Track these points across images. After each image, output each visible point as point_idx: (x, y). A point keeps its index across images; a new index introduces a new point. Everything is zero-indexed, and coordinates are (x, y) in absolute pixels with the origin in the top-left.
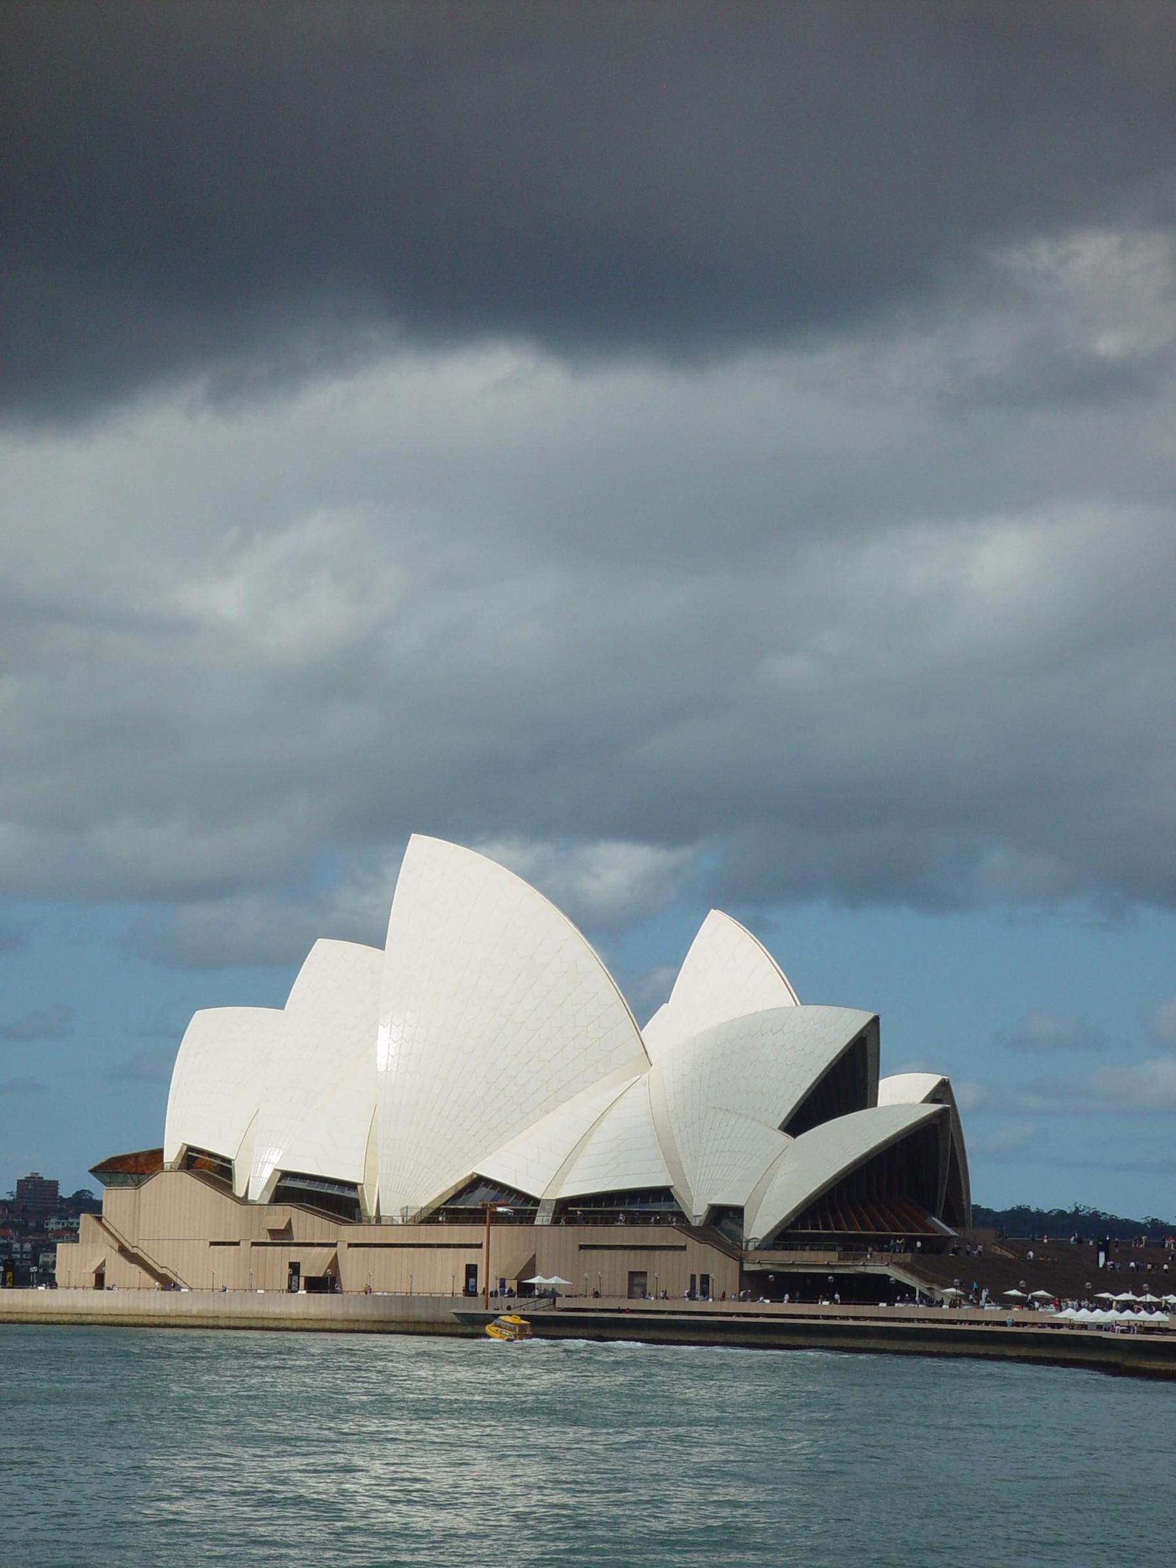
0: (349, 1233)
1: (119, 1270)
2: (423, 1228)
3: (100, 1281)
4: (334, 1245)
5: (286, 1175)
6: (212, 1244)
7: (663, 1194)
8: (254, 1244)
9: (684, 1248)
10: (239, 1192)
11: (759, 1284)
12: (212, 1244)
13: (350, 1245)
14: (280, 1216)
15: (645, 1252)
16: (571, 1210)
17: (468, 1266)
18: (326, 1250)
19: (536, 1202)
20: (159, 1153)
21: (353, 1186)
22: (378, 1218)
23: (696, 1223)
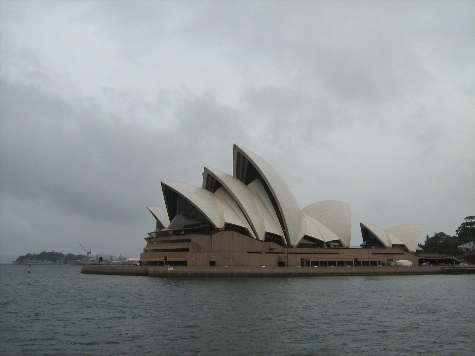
2: (297, 249)
3: (213, 264)
4: (284, 253)
5: (267, 234)
6: (248, 252)
7: (338, 241)
8: (267, 253)
9: (403, 254)
10: (255, 238)
12: (248, 252)
13: (288, 253)
14: (273, 245)
15: (384, 255)
17: (301, 258)
18: (282, 255)
22: (289, 246)
23: (389, 248)
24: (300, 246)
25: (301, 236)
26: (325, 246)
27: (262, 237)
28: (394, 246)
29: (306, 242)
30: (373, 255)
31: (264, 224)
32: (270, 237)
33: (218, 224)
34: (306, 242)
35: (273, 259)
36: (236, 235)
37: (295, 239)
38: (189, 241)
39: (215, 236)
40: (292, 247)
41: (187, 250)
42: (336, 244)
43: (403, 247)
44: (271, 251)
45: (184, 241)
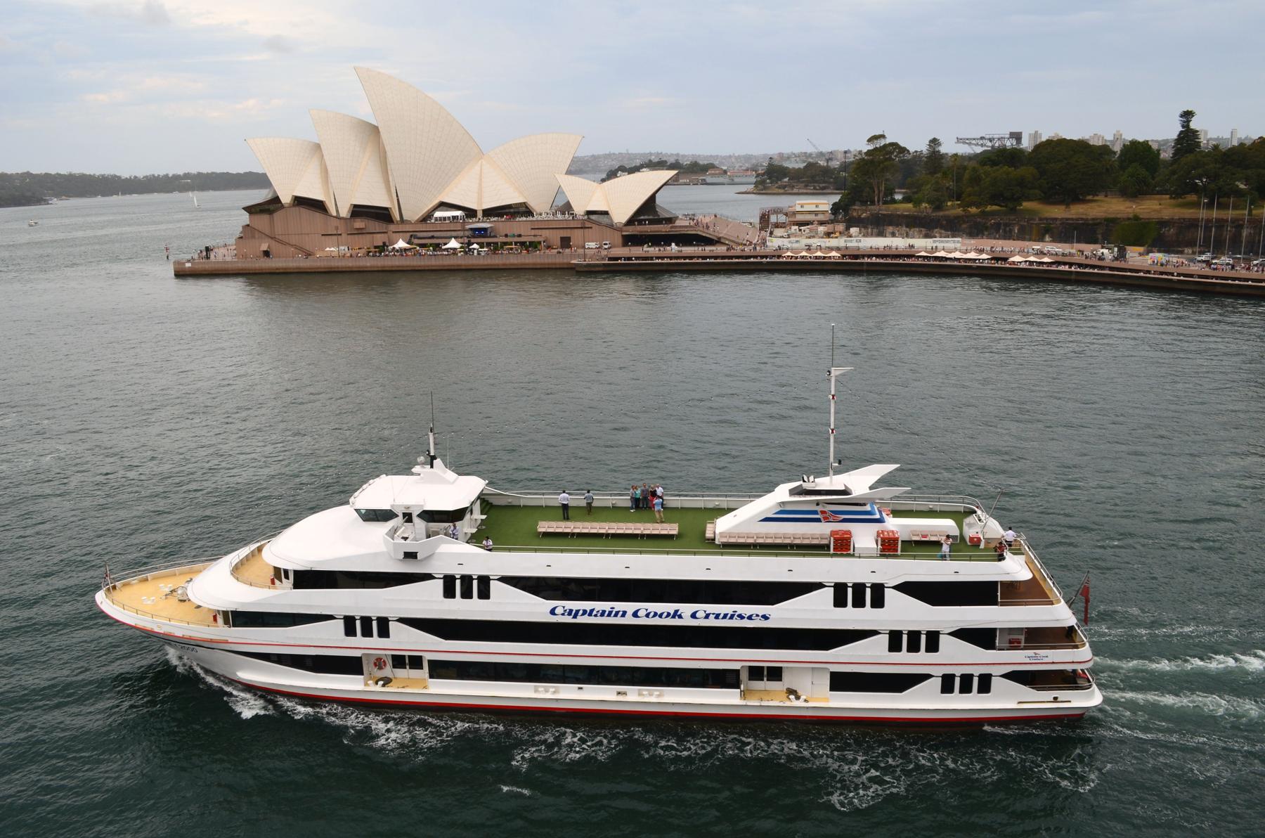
0: (392, 227)
1: (276, 248)
3: (267, 254)
5: (355, 206)
10: (334, 214)
11: (630, 240)
14: (359, 224)
16: (488, 213)
19: (475, 211)
20: (276, 200)
21: (386, 209)
25: (436, 202)
26: (480, 214)
27: (345, 212)
28: (589, 213)
30: (533, 232)
32: (359, 211)
33: (286, 199)
36: (305, 212)
37: (413, 210)
39: (277, 215)
40: (409, 222)
43: (606, 213)
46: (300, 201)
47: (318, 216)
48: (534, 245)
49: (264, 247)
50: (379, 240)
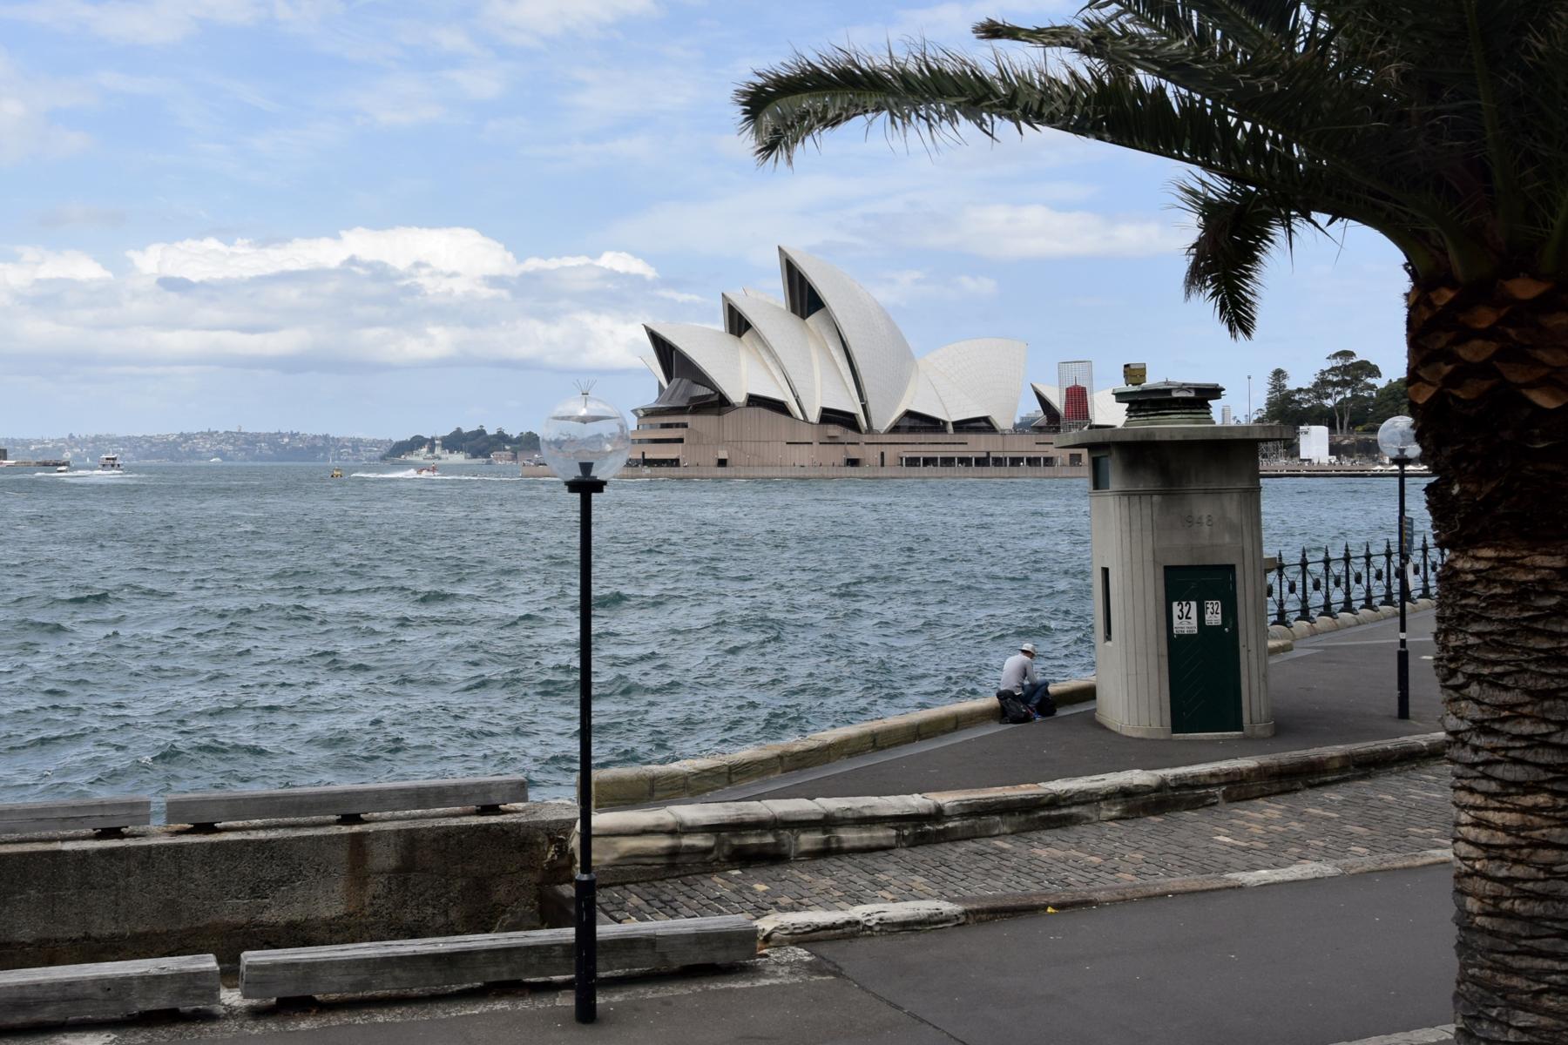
0: (866, 438)
5: (825, 410)
7: (986, 419)
14: (834, 430)
16: (961, 426)
19: (945, 423)
21: (852, 416)
22: (870, 430)
24: (895, 429)
26: (950, 428)
27: (814, 416)
29: (907, 423)
30: (1038, 448)
31: (824, 389)
32: (830, 416)
33: (737, 396)
34: (907, 423)
35: (838, 454)
36: (766, 413)
38: (685, 426)
39: (729, 417)
41: (681, 441)
42: (984, 424)
44: (833, 441)
45: (677, 425)
46: (754, 401)
47: (783, 417)
48: (1049, 461)
49: (723, 455)
50: (854, 452)
